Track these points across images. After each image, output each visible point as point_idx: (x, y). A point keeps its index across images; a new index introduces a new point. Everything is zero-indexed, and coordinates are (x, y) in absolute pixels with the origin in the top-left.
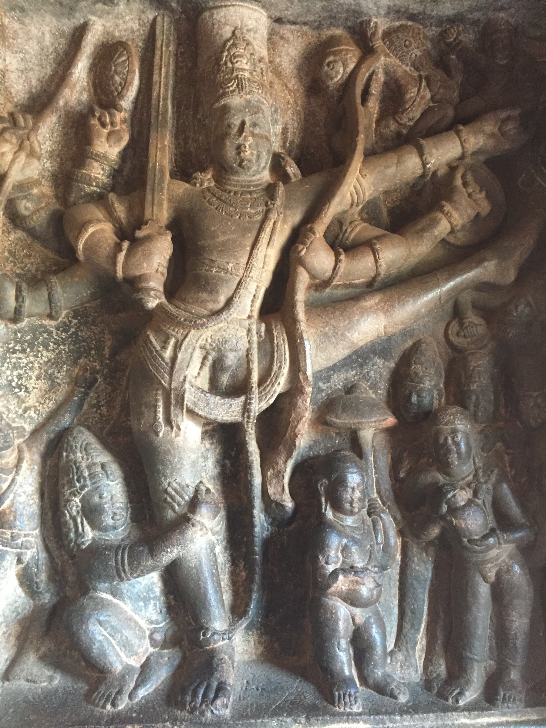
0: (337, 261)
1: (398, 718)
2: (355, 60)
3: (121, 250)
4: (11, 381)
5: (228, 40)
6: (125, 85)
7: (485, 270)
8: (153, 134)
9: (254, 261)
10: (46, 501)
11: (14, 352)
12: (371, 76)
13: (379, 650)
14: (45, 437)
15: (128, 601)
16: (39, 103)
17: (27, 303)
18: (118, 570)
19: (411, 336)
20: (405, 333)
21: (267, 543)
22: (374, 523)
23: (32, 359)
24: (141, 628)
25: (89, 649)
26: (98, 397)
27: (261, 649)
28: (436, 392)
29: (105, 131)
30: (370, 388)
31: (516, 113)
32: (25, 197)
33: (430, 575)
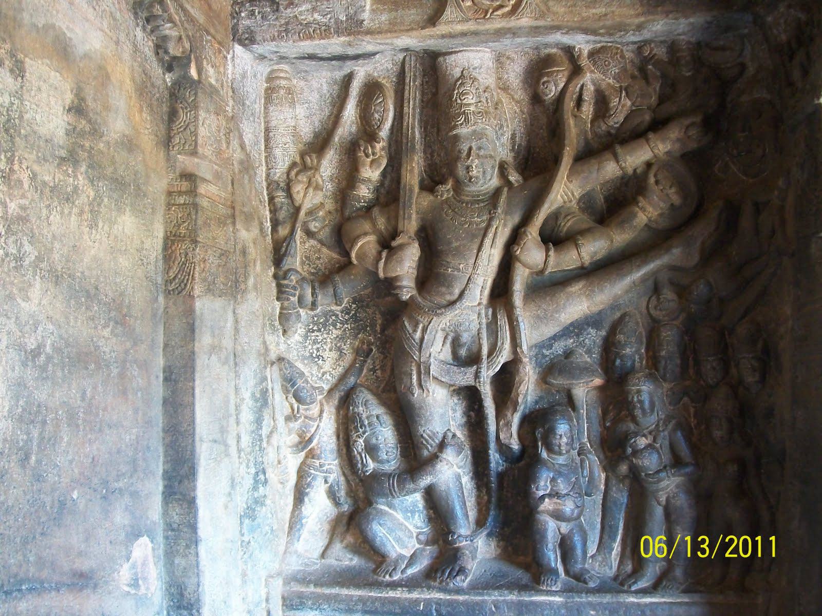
0: (547, 256)
1: (584, 595)
2: (564, 80)
3: (381, 259)
4: (312, 354)
5: (457, 80)
6: (382, 121)
7: (674, 255)
8: (404, 160)
9: (479, 261)
10: (341, 440)
11: (313, 332)
12: (582, 86)
13: (579, 552)
14: (337, 396)
15: (400, 512)
16: (319, 143)
17: (319, 298)
18: (390, 490)
19: (619, 310)
20: (614, 307)
21: (501, 476)
22: (582, 461)
23: (325, 336)
24: (409, 531)
25: (374, 540)
26: (374, 363)
27: (499, 551)
28: (637, 357)
29: (369, 160)
30: (586, 353)
31: (698, 119)
32: (314, 220)
33: (626, 500)
